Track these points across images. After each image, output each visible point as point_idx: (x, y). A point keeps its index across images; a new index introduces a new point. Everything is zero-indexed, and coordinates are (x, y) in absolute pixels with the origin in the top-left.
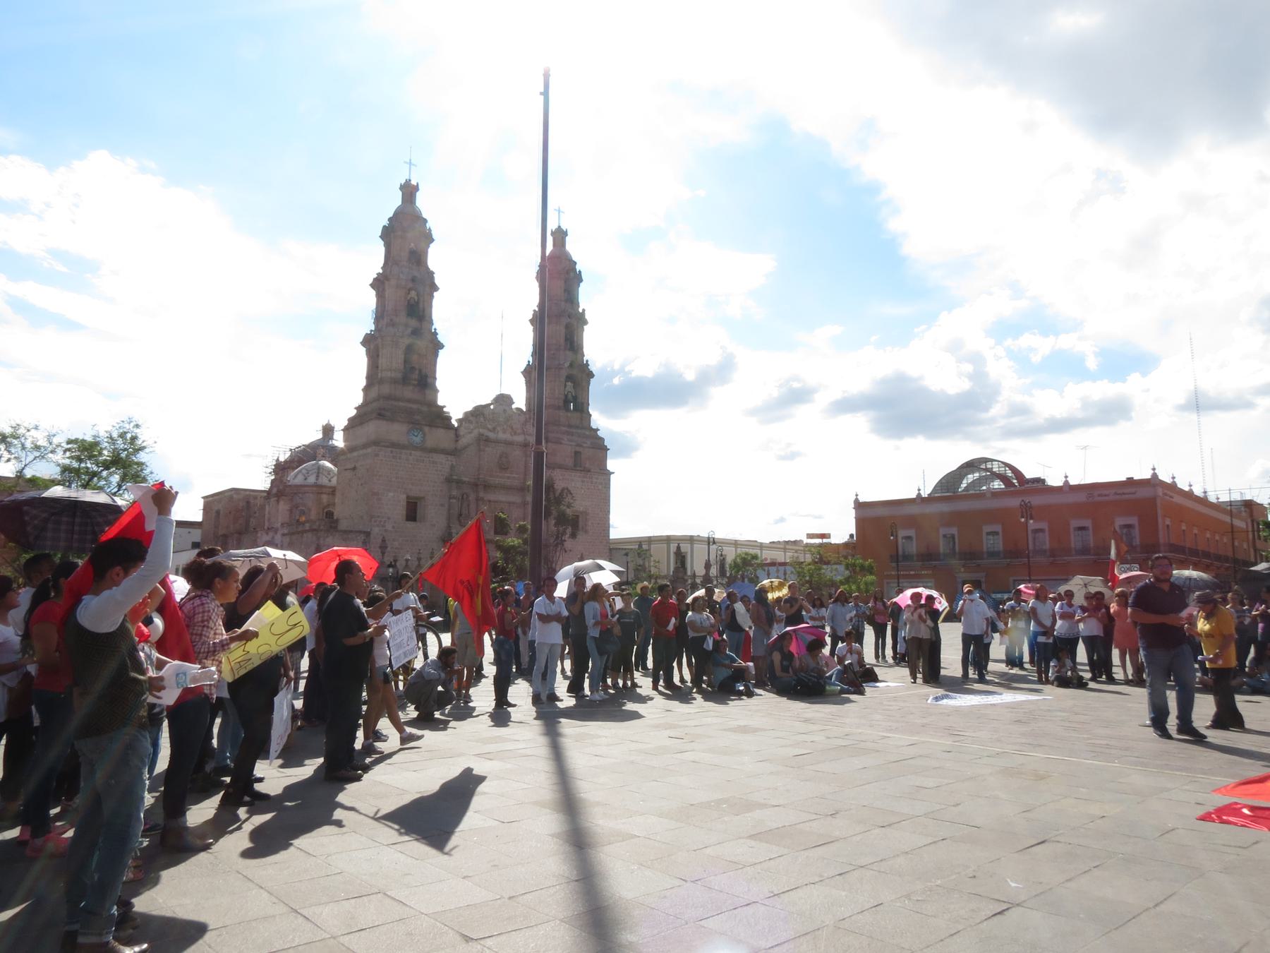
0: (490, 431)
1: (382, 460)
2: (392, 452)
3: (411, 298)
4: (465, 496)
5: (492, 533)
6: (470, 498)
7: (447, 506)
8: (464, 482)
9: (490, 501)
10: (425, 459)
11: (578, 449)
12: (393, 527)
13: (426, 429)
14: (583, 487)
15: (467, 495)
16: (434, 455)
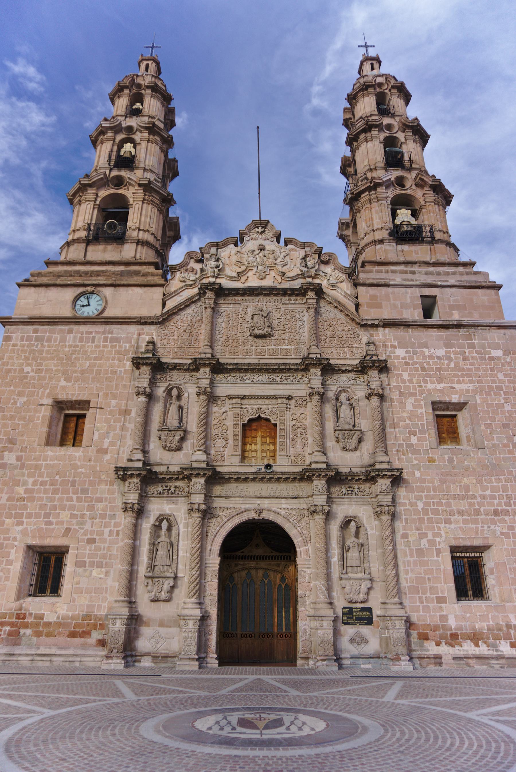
0: (233, 279)
1: (14, 345)
2: (36, 331)
3: (125, 152)
4: (175, 392)
5: (237, 460)
6: (186, 395)
7: (133, 414)
8: (175, 367)
9: (230, 397)
10: (97, 336)
11: (427, 292)
12: (19, 459)
13: (108, 292)
14: (452, 356)
15: (179, 389)
16: (115, 328)
